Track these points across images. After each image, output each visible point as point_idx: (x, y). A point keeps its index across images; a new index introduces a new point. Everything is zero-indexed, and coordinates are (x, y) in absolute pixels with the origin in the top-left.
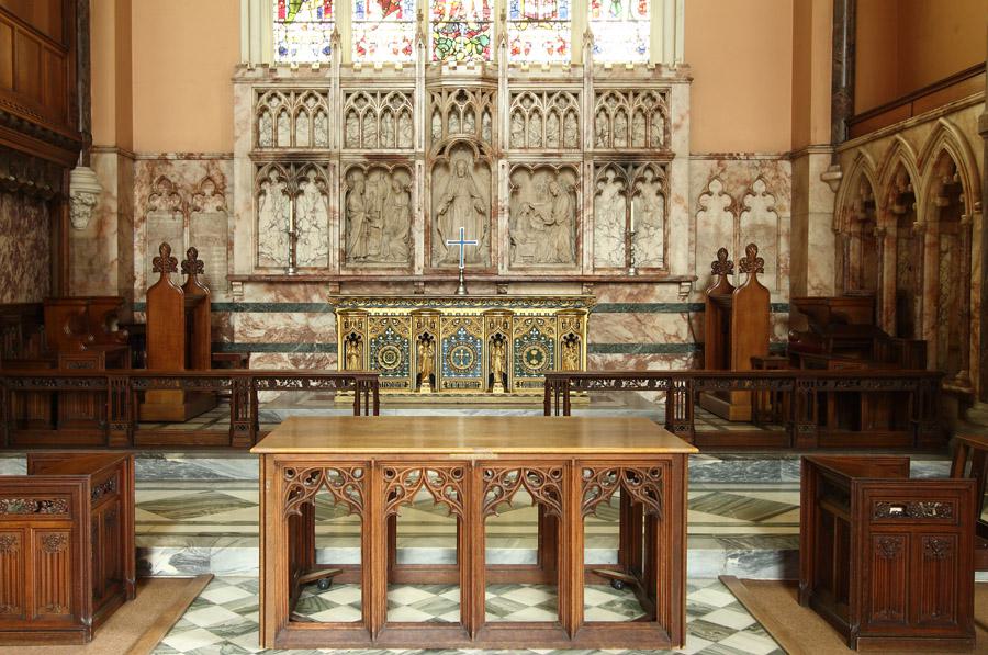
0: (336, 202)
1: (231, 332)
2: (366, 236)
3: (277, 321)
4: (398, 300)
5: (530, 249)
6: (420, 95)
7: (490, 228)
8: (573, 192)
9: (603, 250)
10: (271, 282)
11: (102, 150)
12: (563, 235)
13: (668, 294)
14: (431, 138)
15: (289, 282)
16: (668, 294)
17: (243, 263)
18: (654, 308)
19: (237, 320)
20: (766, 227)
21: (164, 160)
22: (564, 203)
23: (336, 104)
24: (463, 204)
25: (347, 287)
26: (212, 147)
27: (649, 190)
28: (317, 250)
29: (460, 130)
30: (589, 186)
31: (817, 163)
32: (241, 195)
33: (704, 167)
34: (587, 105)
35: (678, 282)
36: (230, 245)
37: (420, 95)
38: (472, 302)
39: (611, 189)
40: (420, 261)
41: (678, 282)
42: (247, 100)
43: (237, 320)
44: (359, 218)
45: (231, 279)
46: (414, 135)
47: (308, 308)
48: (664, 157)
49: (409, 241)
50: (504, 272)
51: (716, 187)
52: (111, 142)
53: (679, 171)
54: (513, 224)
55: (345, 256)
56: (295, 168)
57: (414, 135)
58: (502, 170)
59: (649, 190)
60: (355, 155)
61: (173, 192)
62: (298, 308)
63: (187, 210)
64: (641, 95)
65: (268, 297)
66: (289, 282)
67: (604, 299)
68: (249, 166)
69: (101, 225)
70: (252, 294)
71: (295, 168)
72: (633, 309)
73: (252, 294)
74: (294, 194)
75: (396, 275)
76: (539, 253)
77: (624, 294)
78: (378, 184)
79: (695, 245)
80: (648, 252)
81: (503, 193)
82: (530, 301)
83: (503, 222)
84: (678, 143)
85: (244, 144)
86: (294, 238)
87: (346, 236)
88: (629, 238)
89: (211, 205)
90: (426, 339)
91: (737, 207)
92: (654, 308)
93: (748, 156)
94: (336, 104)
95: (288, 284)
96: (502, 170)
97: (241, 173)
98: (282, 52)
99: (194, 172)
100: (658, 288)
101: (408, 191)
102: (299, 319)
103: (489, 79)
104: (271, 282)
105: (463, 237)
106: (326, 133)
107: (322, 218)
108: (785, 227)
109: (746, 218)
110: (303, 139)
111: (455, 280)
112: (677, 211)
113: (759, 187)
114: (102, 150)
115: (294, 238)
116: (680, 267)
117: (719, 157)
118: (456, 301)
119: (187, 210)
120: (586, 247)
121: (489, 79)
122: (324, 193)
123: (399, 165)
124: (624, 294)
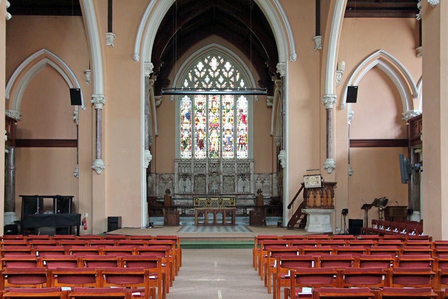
0: (193, 182)
1: (174, 203)
2: (198, 187)
3: (182, 201)
4: (204, 197)
5: (226, 189)
6: (207, 164)
7: (219, 186)
8: (234, 180)
9: (239, 189)
10: (181, 195)
11: (153, 173)
12: (232, 187)
13: (251, 196)
14: (209, 171)
15: (185, 195)
16: (251, 196)
17: (176, 191)
18: (248, 199)
19: (175, 201)
20: (268, 185)
21: (162, 174)
22: (232, 181)
23: (193, 165)
24: (214, 182)
25: (194, 195)
26: (170, 172)
27: (247, 179)
28: (188, 190)
29: (214, 170)
30: (236, 179)
31: (274, 175)
32: (176, 181)
33: (257, 176)
34: (236, 166)
35: (252, 194)
36: (174, 189)
37: (207, 164)
38: (216, 198)
39: (240, 179)
40: (207, 191)
41: (252, 194)
42: (177, 165)
43: (175, 201)
44: (196, 184)
45: (174, 195)
46: (206, 171)
47: (188, 199)
48: (249, 174)
49: (205, 188)
50: (222, 193)
51: (259, 179)
52: (154, 172)
53: (252, 176)
54: (223, 185)
55: (194, 191)
56: (185, 176)
57: (206, 171)
58: (221, 176)
59: (247, 179)
60: (196, 174)
61: (163, 179)
62: (186, 199)
63: (166, 183)
64: (244, 163)
65: (181, 197)
66: (185, 195)
67: (239, 197)
68: (177, 175)
69: (152, 185)
70: (177, 197)
71: (185, 176)
72: (244, 199)
73: (177, 197)
74: (185, 180)
75: (203, 193)
76: (228, 190)
77: (243, 197)
78: (200, 179)
79: (255, 188)
80: (247, 190)
81: (222, 180)
82: (225, 198)
83: (222, 185)
84: (252, 172)
85: (176, 172)
86: (185, 187)
87: (194, 187)
88: (244, 187)
89: (170, 182)
90: (209, 203)
91: (263, 182)
92: (248, 199)
93: (264, 174)
94: (193, 165)
95: (184, 195)
96: (221, 176)
97: (176, 176)
98: (182, 156)
99: (167, 177)
100: (249, 196)
101: (205, 180)
102: (186, 201)
103: (219, 162)
104: (181, 195)
105: (215, 187)
106: (192, 170)
107: (190, 184)
108: (271, 186)
109: (264, 184)
110: (186, 171)
111: (212, 194)
112: (251, 183)
113: (266, 179)
114: (153, 173)
115: (185, 187)
116: (252, 192)
117: (259, 174)
118: (214, 198)
119: (166, 183)
120: (236, 189)
121: (219, 162)
122: (190, 180)
123: (204, 175)
124: (243, 197)
